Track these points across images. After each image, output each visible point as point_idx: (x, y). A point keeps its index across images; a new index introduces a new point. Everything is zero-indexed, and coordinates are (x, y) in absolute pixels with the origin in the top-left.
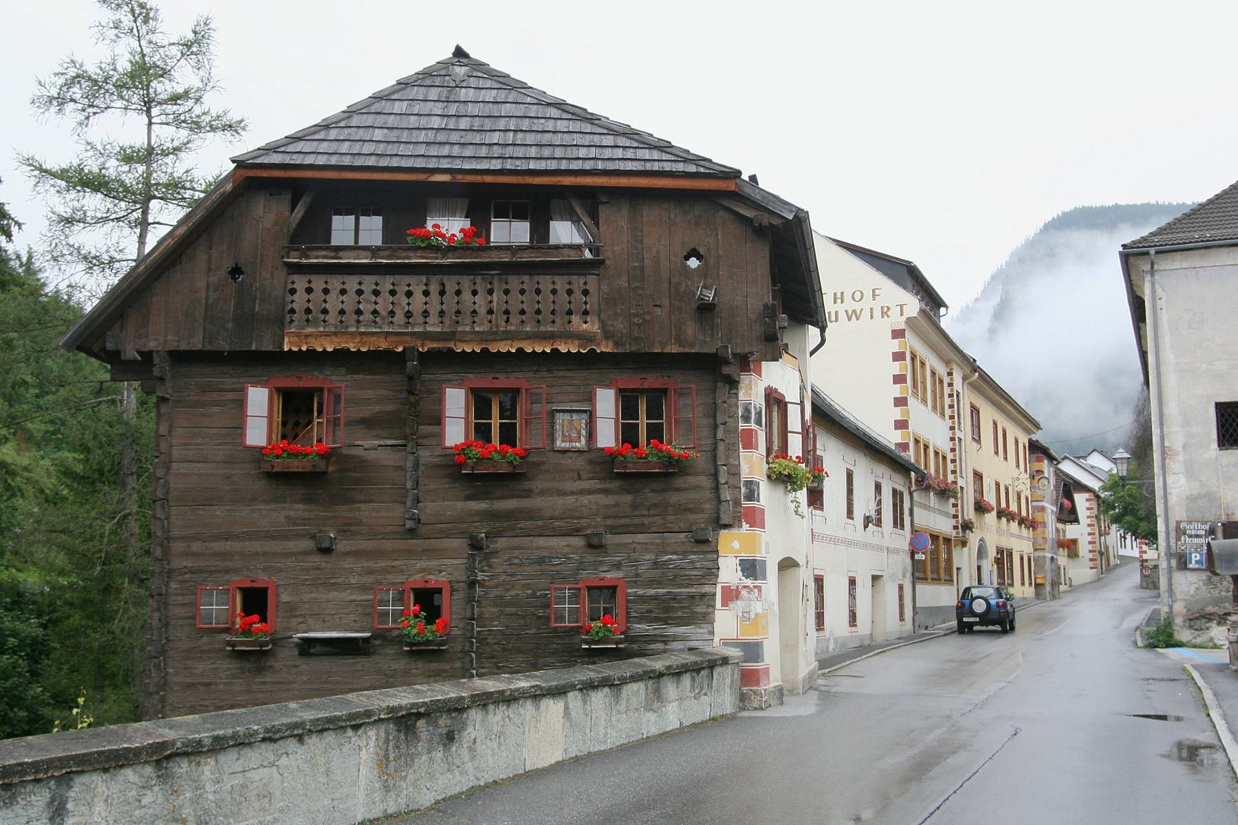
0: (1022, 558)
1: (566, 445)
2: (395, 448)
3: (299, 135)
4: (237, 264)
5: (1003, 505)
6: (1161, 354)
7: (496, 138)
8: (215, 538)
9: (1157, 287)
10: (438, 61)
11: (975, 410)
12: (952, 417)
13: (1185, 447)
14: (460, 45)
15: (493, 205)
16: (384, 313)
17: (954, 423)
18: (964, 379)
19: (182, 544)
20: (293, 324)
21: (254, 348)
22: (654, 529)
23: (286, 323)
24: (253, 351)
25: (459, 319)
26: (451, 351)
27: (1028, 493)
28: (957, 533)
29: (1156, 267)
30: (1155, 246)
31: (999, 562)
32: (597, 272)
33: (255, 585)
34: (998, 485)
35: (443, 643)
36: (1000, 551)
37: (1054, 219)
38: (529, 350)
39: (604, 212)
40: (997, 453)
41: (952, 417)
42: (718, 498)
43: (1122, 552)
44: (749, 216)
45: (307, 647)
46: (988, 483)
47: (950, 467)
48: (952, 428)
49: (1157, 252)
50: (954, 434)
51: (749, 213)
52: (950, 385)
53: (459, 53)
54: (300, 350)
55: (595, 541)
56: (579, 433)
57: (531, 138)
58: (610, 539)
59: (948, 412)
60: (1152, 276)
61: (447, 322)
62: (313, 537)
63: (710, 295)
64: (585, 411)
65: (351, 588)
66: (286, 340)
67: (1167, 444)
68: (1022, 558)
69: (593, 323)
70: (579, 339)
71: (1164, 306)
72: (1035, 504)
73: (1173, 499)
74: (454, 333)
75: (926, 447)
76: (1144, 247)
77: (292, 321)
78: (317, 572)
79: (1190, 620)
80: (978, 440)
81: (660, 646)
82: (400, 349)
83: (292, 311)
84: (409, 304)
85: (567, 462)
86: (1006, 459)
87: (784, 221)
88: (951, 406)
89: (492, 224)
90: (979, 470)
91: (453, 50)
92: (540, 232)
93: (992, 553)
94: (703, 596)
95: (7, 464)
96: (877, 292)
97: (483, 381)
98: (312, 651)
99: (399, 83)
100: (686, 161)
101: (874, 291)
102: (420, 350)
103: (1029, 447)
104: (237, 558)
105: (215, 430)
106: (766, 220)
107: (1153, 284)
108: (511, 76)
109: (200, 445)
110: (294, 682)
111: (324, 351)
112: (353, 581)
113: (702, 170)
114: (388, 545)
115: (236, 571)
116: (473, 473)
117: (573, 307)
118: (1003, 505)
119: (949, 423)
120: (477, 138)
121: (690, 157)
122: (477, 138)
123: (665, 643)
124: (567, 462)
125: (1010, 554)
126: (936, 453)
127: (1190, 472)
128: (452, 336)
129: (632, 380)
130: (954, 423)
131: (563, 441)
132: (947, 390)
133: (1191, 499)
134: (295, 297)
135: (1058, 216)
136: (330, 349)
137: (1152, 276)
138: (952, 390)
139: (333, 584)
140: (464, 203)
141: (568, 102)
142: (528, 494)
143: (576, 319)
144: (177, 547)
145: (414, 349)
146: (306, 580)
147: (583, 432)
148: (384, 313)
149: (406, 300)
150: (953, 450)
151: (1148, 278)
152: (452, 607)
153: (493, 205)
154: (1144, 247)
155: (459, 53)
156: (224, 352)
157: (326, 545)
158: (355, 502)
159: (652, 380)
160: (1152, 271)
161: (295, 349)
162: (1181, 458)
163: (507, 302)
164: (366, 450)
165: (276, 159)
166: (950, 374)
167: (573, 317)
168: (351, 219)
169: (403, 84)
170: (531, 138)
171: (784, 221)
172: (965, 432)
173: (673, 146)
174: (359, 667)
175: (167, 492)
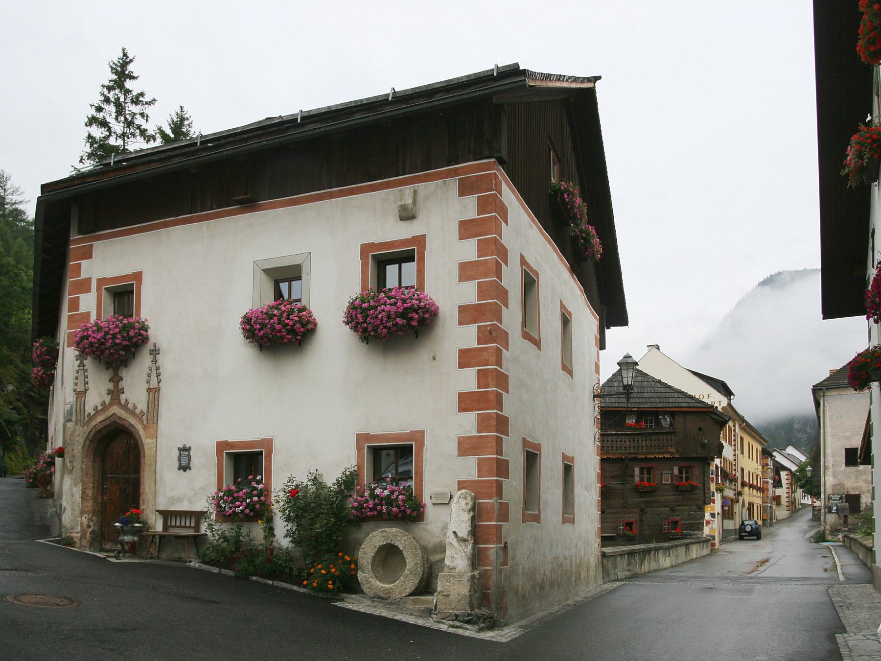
0: (758, 507)
5: (751, 483)
6: (826, 429)
9: (825, 402)
11: (742, 439)
12: (735, 445)
13: (833, 465)
17: (735, 448)
18: (739, 426)
26: (637, 457)
27: (761, 475)
28: (736, 497)
29: (825, 394)
30: (825, 386)
31: (749, 509)
34: (749, 472)
36: (750, 504)
37: (764, 280)
40: (749, 457)
41: (735, 445)
42: (705, 496)
43: (803, 502)
46: (746, 472)
47: (734, 468)
48: (735, 450)
49: (826, 389)
50: (735, 453)
51: (715, 417)
52: (734, 431)
55: (673, 509)
58: (677, 508)
59: (733, 443)
60: (824, 398)
67: (826, 464)
68: (758, 507)
71: (828, 410)
72: (764, 480)
73: (827, 486)
75: (727, 461)
76: (821, 387)
79: (832, 532)
80: (742, 453)
81: (690, 537)
82: (624, 457)
85: (665, 487)
86: (752, 459)
88: (734, 440)
90: (743, 467)
93: (747, 505)
94: (701, 523)
96: (710, 395)
97: (644, 465)
101: (708, 395)
103: (762, 451)
107: (824, 402)
112: (610, 520)
113: (704, 406)
117: (668, 444)
118: (751, 483)
119: (733, 448)
123: (691, 536)
125: (753, 506)
126: (729, 462)
127: (834, 475)
129: (682, 464)
130: (735, 448)
132: (733, 433)
133: (835, 486)
135: (767, 277)
137: (824, 398)
138: (735, 433)
149: (624, 443)
150: (735, 460)
151: (822, 398)
152: (635, 527)
154: (821, 387)
159: (688, 464)
160: (824, 396)
162: (831, 470)
166: (734, 426)
172: (738, 452)
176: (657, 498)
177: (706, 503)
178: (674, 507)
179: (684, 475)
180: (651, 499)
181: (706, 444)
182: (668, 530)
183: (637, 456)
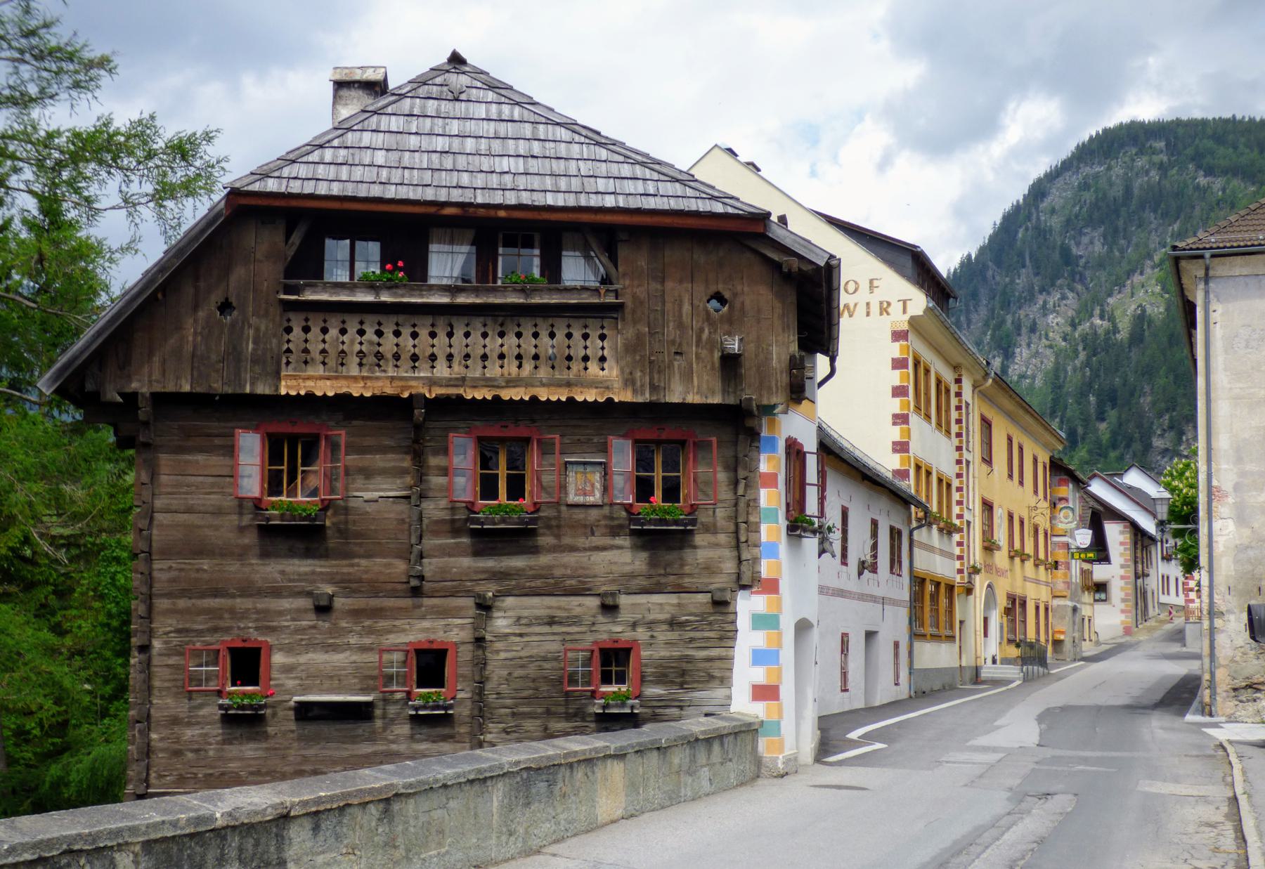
0: (1037, 608)
1: (580, 499)
3: (291, 156)
4: (227, 299)
6: (1213, 377)
7: (505, 164)
8: (203, 595)
9: (1211, 296)
10: (432, 66)
11: (986, 424)
12: (959, 435)
13: (1237, 487)
16: (389, 356)
17: (961, 442)
18: (975, 387)
19: (166, 601)
20: (290, 367)
21: (248, 390)
22: (669, 589)
23: (283, 366)
25: (468, 362)
26: (460, 398)
27: (1048, 526)
28: (962, 578)
29: (1211, 273)
30: (1211, 248)
31: (1008, 611)
32: (615, 316)
33: (247, 645)
34: (1011, 517)
35: (451, 707)
36: (1012, 598)
38: (543, 399)
39: (623, 252)
40: (1011, 476)
41: (959, 435)
42: (739, 558)
44: (777, 259)
45: (305, 712)
46: (1000, 515)
47: (956, 496)
48: (959, 449)
49: (1213, 256)
50: (961, 455)
51: (775, 256)
52: (959, 394)
53: (456, 60)
54: (298, 394)
55: (609, 601)
56: (593, 485)
57: (545, 166)
58: (624, 600)
59: (954, 428)
60: (1207, 283)
61: (456, 367)
62: (309, 594)
63: (734, 345)
64: (600, 463)
66: (283, 383)
67: (1215, 483)
68: (1037, 608)
69: (611, 369)
70: (596, 388)
71: (1218, 319)
72: (1055, 539)
73: (1219, 548)
74: (463, 379)
75: (929, 473)
76: (1198, 249)
77: (288, 363)
78: (314, 631)
79: (1235, 690)
80: (988, 460)
81: (675, 711)
82: (406, 395)
83: (289, 351)
84: (414, 346)
85: (579, 515)
86: (1021, 483)
88: (959, 421)
89: (500, 259)
90: (989, 497)
91: (448, 55)
92: (552, 270)
93: (1002, 602)
94: (720, 659)
96: (876, 283)
97: (493, 430)
98: (310, 715)
100: (713, 198)
101: (871, 281)
102: (428, 396)
103: (1051, 467)
104: (226, 616)
105: (200, 479)
106: (795, 264)
107: (1207, 293)
108: (515, 88)
109: (184, 493)
110: (288, 748)
111: (325, 395)
112: (352, 641)
113: (730, 210)
115: (227, 630)
116: (482, 529)
117: (589, 352)
119: (956, 442)
120: (486, 164)
121: (716, 194)
122: (486, 164)
123: (681, 708)
124: (579, 515)
125: (1024, 604)
126: (940, 481)
127: (1241, 518)
128: (462, 381)
130: (961, 442)
131: (576, 495)
132: (954, 402)
133: (1241, 549)
134: (291, 336)
136: (330, 394)
137: (1207, 283)
138: (960, 401)
139: (330, 645)
140: (470, 234)
141: (579, 122)
142: (535, 550)
143: (593, 368)
144: (162, 604)
146: (302, 640)
147: (598, 485)
148: (389, 356)
149: (411, 342)
150: (959, 476)
151: (1201, 286)
152: (459, 666)
153: (501, 236)
154: (1198, 249)
155: (456, 60)
156: (216, 395)
157: (324, 602)
159: (670, 431)
160: (1207, 279)
161: (293, 393)
162: (1230, 500)
163: (519, 346)
164: (366, 501)
165: (272, 185)
166: (958, 381)
167: (589, 364)
170: (545, 166)
172: (974, 454)
173: (696, 181)
174: (360, 731)
175: (150, 546)
176: (544, 560)
177: (744, 582)
178: (613, 594)
179: (658, 475)
180: (518, 562)
181: (739, 355)
182: (589, 684)
183: (461, 391)
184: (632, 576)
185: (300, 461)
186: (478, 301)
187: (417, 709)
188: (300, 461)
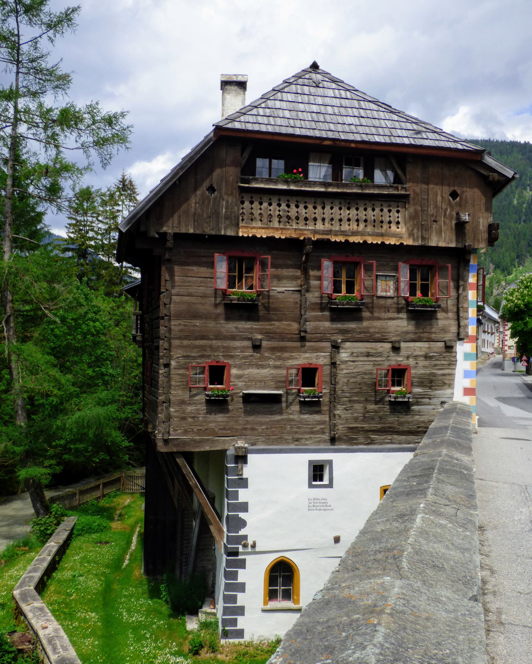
1: (384, 294)
2: (295, 292)
3: (243, 111)
4: (212, 185)
7: (350, 120)
8: (196, 339)
10: (303, 68)
14: (317, 61)
15: (344, 159)
16: (294, 218)
19: (177, 341)
20: (244, 222)
21: (223, 233)
22: (425, 340)
23: (240, 221)
24: (222, 235)
25: (333, 222)
26: (329, 240)
32: (404, 201)
33: (218, 364)
35: (321, 397)
38: (370, 242)
39: (409, 168)
43: (483, 350)
44: (486, 174)
45: (248, 399)
53: (315, 66)
54: (248, 236)
55: (397, 345)
56: (389, 287)
57: (369, 122)
58: (403, 345)
61: (327, 224)
62: (250, 339)
63: (465, 217)
64: (394, 276)
65: (270, 367)
66: (241, 230)
69: (402, 228)
70: (395, 237)
74: (331, 231)
77: (243, 220)
78: (252, 358)
82: (302, 238)
83: (243, 213)
84: (306, 213)
87: (505, 178)
89: (344, 169)
91: (311, 63)
94: (449, 375)
95: (407, 312)
98: (251, 400)
99: (285, 82)
100: (455, 141)
102: (313, 239)
104: (208, 349)
105: (195, 279)
106: (496, 176)
108: (345, 82)
109: (188, 286)
110: (240, 417)
111: (261, 237)
112: (271, 363)
114: (290, 344)
115: (208, 357)
116: (338, 308)
117: (391, 219)
120: (340, 119)
121: (456, 139)
122: (340, 119)
123: (430, 398)
124: (382, 302)
128: (330, 232)
129: (417, 261)
131: (381, 292)
134: (244, 206)
136: (264, 236)
139: (260, 365)
140: (328, 157)
141: (380, 101)
142: (360, 319)
143: (394, 227)
144: (176, 343)
145: (310, 239)
146: (246, 362)
147: (392, 287)
148: (294, 218)
153: (344, 159)
155: (315, 66)
156: (206, 235)
157: (258, 344)
158: (272, 321)
159: (428, 261)
161: (246, 235)
163: (357, 215)
164: (278, 292)
165: (237, 125)
167: (392, 225)
168: (267, 161)
169: (287, 83)
170: (369, 122)
171: (505, 178)
173: (444, 132)
174: (275, 409)
175: (170, 313)
176: (365, 324)
177: (461, 337)
178: (399, 342)
179: (419, 282)
180: (352, 325)
181: (467, 222)
182: (386, 386)
183: (329, 237)
184: (407, 333)
185: (244, 271)
186: (339, 191)
187: (304, 398)
188: (244, 271)
